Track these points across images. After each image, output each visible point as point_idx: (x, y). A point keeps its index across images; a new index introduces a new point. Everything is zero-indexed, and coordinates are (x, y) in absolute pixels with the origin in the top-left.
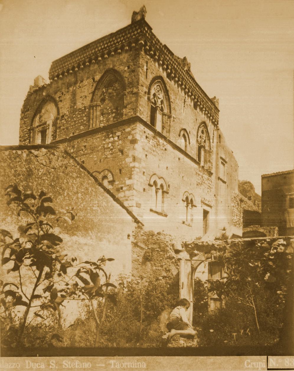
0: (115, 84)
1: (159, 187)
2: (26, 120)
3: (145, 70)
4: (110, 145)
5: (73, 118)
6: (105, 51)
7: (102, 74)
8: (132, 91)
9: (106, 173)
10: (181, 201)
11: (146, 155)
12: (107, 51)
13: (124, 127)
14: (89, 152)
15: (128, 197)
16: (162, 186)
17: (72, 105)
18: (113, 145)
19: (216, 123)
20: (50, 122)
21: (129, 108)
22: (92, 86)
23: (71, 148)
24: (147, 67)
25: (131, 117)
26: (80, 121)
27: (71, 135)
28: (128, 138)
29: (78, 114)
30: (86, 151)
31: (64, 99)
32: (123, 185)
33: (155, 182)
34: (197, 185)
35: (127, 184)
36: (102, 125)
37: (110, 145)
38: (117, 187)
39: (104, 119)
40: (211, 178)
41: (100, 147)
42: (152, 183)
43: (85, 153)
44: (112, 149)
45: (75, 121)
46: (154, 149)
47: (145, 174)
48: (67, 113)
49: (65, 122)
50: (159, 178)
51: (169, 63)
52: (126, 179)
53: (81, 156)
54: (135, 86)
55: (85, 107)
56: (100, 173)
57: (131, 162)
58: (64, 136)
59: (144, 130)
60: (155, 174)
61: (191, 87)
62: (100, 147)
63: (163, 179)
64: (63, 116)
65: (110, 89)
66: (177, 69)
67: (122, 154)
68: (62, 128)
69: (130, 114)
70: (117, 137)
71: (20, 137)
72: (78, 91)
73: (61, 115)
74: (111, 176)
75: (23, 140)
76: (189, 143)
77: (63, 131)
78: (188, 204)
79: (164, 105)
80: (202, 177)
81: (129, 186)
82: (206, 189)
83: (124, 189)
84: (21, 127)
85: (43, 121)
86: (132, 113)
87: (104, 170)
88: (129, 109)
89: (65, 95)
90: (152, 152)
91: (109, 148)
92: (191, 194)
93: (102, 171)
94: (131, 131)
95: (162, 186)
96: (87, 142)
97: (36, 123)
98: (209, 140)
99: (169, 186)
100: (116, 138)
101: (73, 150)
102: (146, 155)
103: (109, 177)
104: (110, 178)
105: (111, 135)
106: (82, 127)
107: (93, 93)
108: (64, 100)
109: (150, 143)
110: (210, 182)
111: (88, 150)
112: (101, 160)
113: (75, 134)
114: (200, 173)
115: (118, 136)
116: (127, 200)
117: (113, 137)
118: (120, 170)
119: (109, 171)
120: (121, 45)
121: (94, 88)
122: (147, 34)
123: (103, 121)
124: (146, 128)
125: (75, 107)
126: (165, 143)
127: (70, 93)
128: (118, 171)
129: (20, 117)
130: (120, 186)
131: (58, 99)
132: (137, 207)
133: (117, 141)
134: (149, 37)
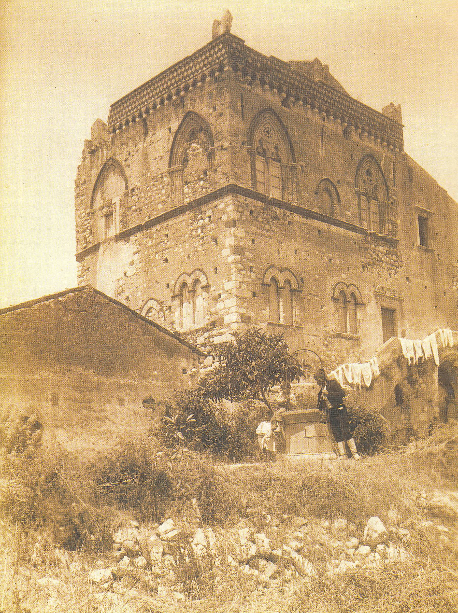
0: (200, 135)
1: (281, 285)
2: (83, 198)
3: (240, 108)
4: (200, 230)
5: (147, 192)
6: (180, 85)
7: (180, 122)
8: (222, 146)
9: (197, 275)
10: (331, 300)
11: (253, 240)
12: (184, 84)
13: (216, 203)
14: (173, 243)
15: (229, 308)
16: (287, 282)
17: (144, 171)
18: (204, 230)
19: (398, 150)
20: (116, 200)
21: (221, 173)
22: (169, 139)
23: (148, 239)
24: (242, 103)
25: (223, 186)
26: (157, 196)
27: (147, 219)
28: (222, 219)
29: (154, 185)
30: (168, 243)
31: (134, 163)
32: (221, 292)
33: (274, 279)
34: (363, 267)
35: (226, 289)
36: (187, 200)
37: (200, 230)
38: (213, 295)
39: (190, 191)
40: (395, 250)
41: (187, 235)
42: (268, 281)
43: (168, 246)
44: (203, 238)
45: (150, 197)
46: (267, 227)
47: (254, 269)
48: (139, 184)
49: (137, 200)
50: (281, 272)
51: (282, 82)
52: (224, 281)
53: (163, 250)
54: (226, 138)
55: (162, 174)
56: (189, 275)
57: (228, 256)
58: (137, 222)
59: (245, 203)
60: (272, 266)
61: (334, 105)
62: (187, 235)
63: (290, 271)
64: (133, 190)
65: (193, 143)
66: (300, 85)
68: (133, 208)
69: (221, 181)
70: (208, 218)
71: (77, 227)
72: (151, 149)
73: (131, 187)
74: (205, 278)
75: (81, 230)
76: (339, 200)
77: (135, 214)
78: (345, 301)
79: (281, 152)
80: (374, 252)
81: (229, 292)
82: (385, 271)
83: (223, 296)
84: (77, 210)
85: (107, 199)
86: (225, 180)
87: (195, 270)
88: (220, 175)
89: (133, 156)
90: (264, 232)
91: (199, 236)
92: (351, 284)
93: (192, 273)
94: (224, 208)
95: (287, 282)
96: (168, 229)
97: (98, 204)
98: (385, 182)
99: (302, 280)
100: (207, 220)
101: (152, 242)
102: (253, 240)
103: (201, 281)
104: (203, 282)
105: (199, 216)
106: (160, 206)
107: (171, 152)
108: (132, 164)
109: (260, 219)
110: (394, 257)
111: (172, 241)
112: (189, 255)
113: (152, 218)
114: (367, 245)
115: (210, 217)
116: (228, 313)
117: (202, 219)
118: (216, 269)
119: (201, 271)
120: (201, 75)
121: (170, 144)
122: (236, 52)
123: (188, 193)
124: (249, 199)
125: (149, 175)
126: (288, 213)
127: (140, 153)
128: (212, 270)
129: (74, 194)
130: (219, 292)
131: (123, 163)
132: (242, 322)
133: (209, 225)
134: (241, 55)
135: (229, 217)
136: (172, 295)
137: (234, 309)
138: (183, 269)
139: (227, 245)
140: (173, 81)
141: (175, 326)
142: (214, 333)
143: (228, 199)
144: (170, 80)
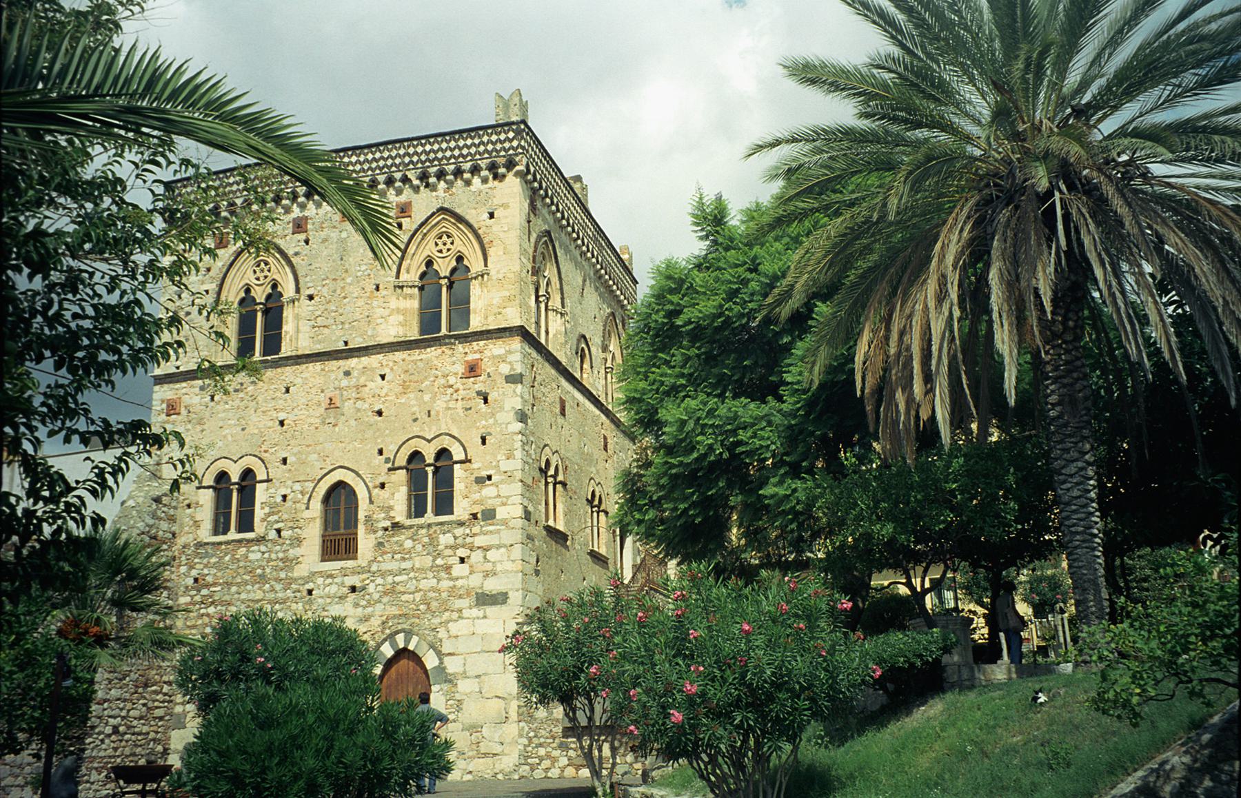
15: (507, 498)
35: (503, 468)
56: (429, 441)
67: (486, 401)
116: (504, 504)
135: (512, 369)
136: (390, 465)
137: (518, 499)
138: (416, 430)
139: (507, 407)
140: (415, 159)
141: (392, 514)
142: (476, 529)
143: (516, 343)
144: (407, 154)
